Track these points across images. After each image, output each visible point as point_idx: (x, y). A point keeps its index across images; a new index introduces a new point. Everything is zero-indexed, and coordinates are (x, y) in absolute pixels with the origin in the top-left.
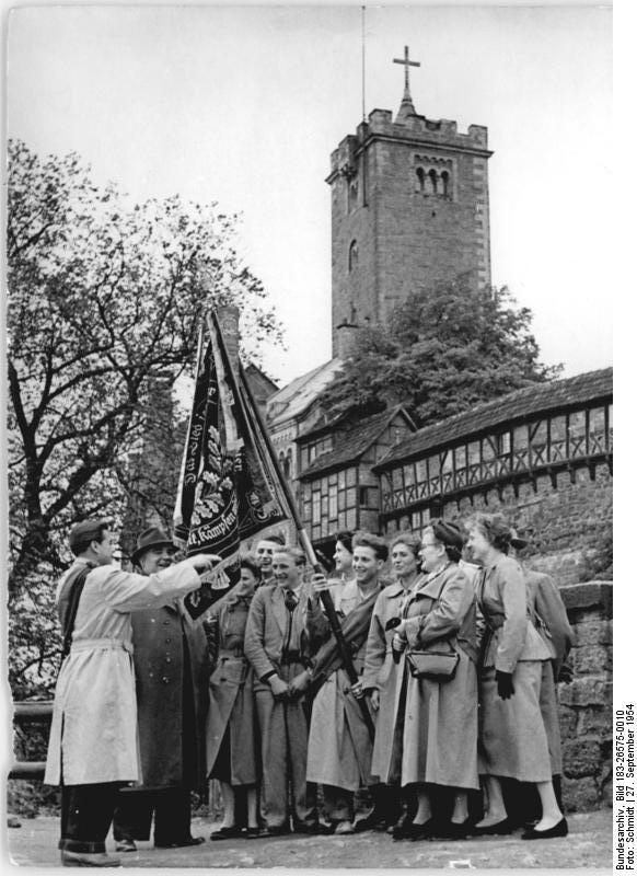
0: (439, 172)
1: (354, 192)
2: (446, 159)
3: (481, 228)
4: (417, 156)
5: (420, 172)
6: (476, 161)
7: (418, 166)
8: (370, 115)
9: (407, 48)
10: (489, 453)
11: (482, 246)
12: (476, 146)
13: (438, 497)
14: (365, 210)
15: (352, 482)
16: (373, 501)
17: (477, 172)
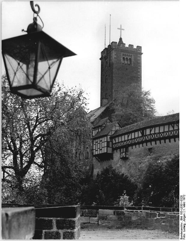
0: (129, 58)
1: (107, 62)
2: (130, 55)
3: (139, 73)
4: (123, 54)
5: (124, 58)
6: (138, 55)
7: (124, 56)
8: (111, 43)
9: (121, 25)
10: (140, 135)
11: (139, 78)
12: (138, 51)
13: (127, 144)
14: (110, 68)
15: (106, 141)
16: (111, 146)
17: (138, 58)
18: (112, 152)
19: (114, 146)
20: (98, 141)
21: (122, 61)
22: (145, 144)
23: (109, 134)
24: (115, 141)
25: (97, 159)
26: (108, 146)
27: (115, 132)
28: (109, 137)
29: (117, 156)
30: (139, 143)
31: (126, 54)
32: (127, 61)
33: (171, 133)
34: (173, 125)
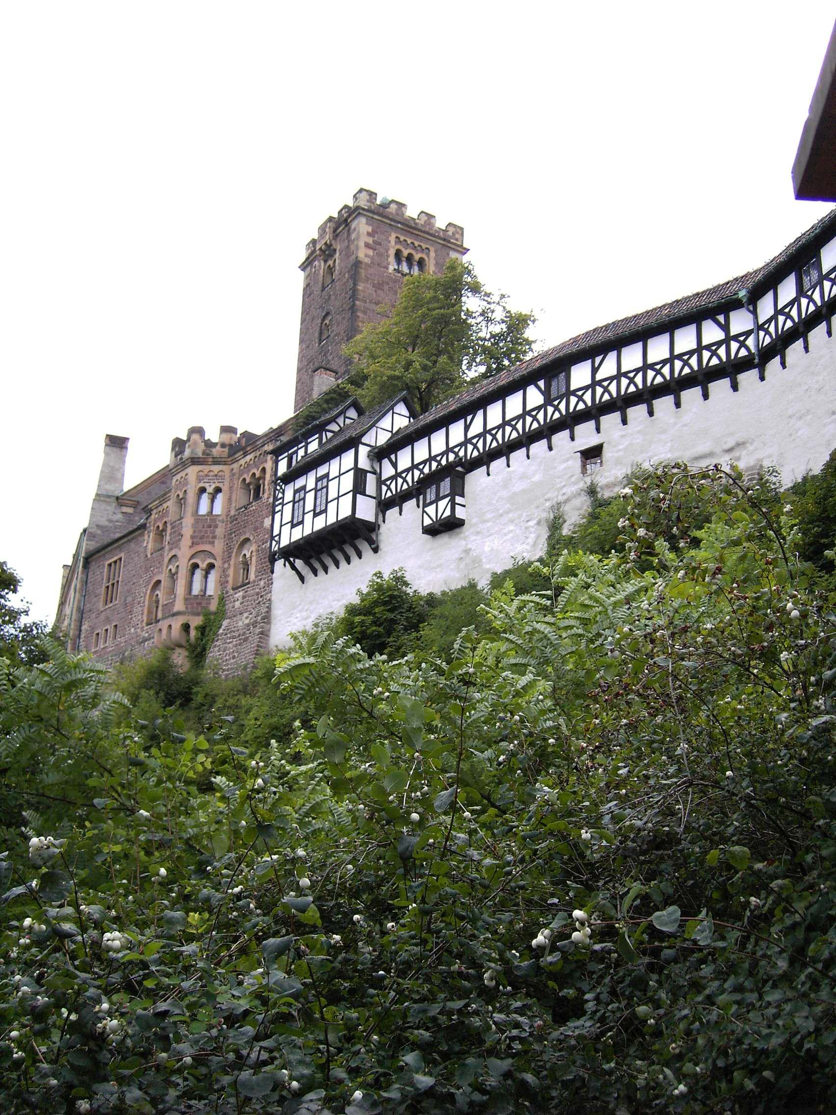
0: (417, 257)
2: (424, 246)
5: (398, 254)
18: (377, 518)
19: (384, 488)
20: (310, 480)
21: (392, 259)
22: (561, 438)
23: (364, 440)
24: (395, 465)
25: (293, 567)
26: (359, 488)
27: (390, 435)
28: (363, 451)
29: (403, 528)
30: (527, 440)
31: (409, 242)
32: (410, 266)
33: (714, 353)
34: (721, 318)
